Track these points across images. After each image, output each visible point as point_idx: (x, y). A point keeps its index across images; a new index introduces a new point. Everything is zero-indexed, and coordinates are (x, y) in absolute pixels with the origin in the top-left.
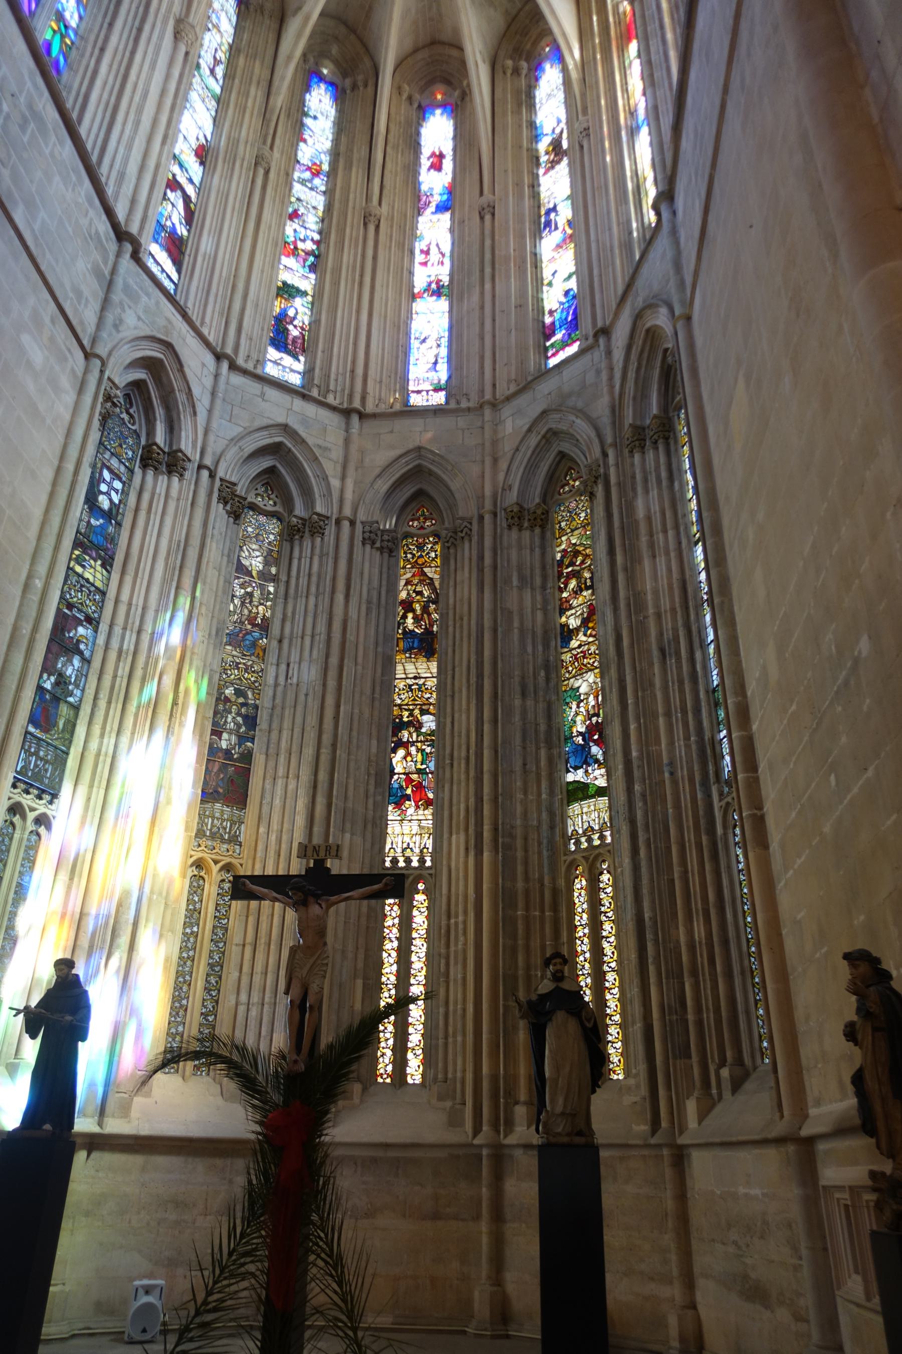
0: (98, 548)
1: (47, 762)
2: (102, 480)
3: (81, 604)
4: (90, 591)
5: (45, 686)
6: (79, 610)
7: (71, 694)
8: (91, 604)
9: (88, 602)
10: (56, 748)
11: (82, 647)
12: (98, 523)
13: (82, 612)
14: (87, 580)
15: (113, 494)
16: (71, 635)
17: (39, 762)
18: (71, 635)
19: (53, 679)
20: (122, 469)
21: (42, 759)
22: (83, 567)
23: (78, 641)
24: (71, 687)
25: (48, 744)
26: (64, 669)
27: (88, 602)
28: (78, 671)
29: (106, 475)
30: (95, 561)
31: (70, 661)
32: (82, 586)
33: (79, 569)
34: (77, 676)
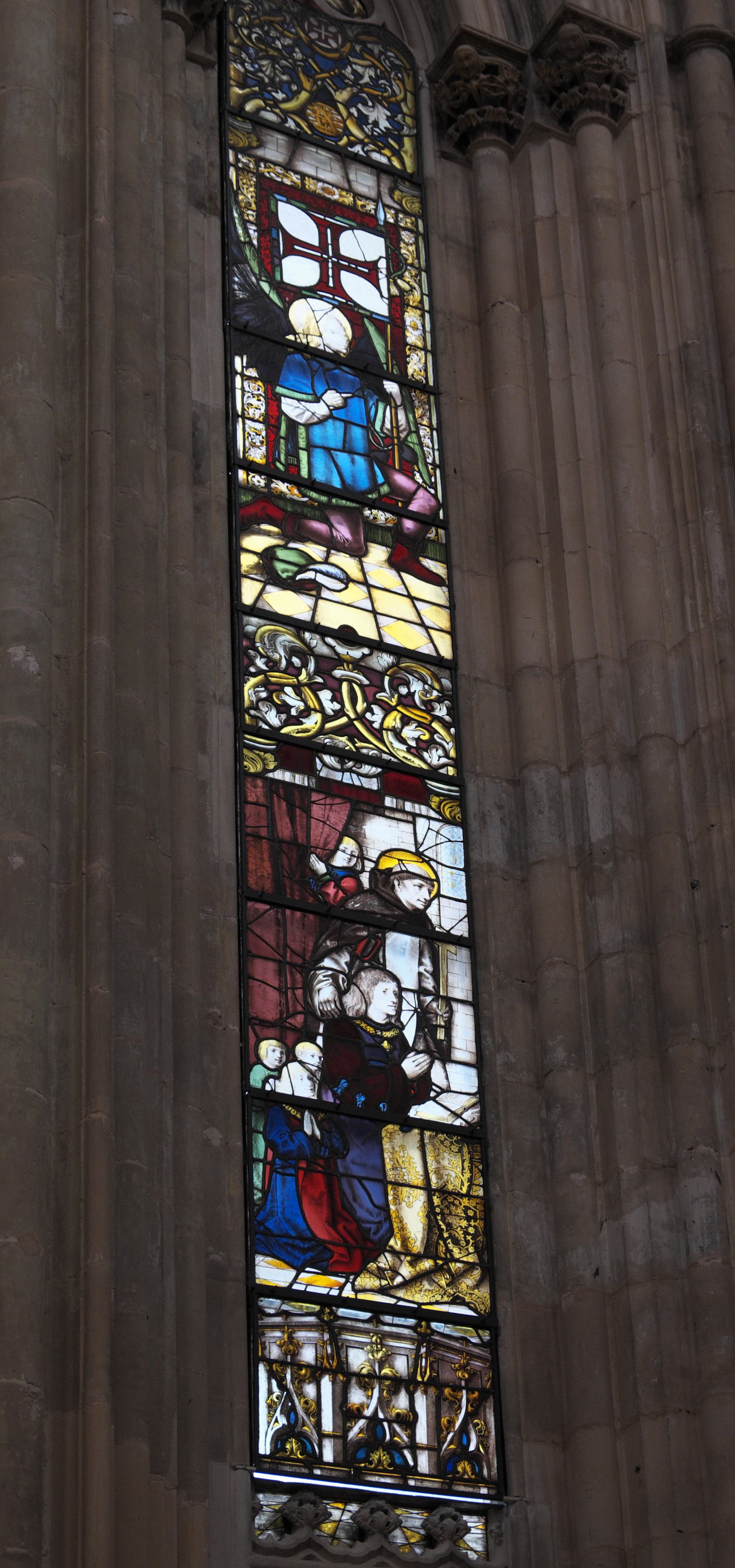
0: (352, 501)
1: (396, 1384)
2: (276, 245)
3: (347, 730)
4: (375, 676)
5: (283, 1087)
6: (342, 755)
7: (422, 1088)
8: (393, 720)
9: (376, 716)
10: (420, 1314)
11: (410, 894)
12: (321, 410)
13: (361, 759)
14: (347, 635)
15: (356, 287)
16: (340, 860)
17: (356, 1397)
18: (340, 860)
19: (309, 1052)
20: (364, 182)
21: (366, 1381)
22: (312, 589)
23: (384, 879)
25: (377, 1310)
26: (352, 1001)
27: (376, 716)
28: (421, 991)
29: (295, 221)
30: (359, 553)
31: (371, 959)
32: (326, 664)
33: (289, 603)
34: (423, 1015)
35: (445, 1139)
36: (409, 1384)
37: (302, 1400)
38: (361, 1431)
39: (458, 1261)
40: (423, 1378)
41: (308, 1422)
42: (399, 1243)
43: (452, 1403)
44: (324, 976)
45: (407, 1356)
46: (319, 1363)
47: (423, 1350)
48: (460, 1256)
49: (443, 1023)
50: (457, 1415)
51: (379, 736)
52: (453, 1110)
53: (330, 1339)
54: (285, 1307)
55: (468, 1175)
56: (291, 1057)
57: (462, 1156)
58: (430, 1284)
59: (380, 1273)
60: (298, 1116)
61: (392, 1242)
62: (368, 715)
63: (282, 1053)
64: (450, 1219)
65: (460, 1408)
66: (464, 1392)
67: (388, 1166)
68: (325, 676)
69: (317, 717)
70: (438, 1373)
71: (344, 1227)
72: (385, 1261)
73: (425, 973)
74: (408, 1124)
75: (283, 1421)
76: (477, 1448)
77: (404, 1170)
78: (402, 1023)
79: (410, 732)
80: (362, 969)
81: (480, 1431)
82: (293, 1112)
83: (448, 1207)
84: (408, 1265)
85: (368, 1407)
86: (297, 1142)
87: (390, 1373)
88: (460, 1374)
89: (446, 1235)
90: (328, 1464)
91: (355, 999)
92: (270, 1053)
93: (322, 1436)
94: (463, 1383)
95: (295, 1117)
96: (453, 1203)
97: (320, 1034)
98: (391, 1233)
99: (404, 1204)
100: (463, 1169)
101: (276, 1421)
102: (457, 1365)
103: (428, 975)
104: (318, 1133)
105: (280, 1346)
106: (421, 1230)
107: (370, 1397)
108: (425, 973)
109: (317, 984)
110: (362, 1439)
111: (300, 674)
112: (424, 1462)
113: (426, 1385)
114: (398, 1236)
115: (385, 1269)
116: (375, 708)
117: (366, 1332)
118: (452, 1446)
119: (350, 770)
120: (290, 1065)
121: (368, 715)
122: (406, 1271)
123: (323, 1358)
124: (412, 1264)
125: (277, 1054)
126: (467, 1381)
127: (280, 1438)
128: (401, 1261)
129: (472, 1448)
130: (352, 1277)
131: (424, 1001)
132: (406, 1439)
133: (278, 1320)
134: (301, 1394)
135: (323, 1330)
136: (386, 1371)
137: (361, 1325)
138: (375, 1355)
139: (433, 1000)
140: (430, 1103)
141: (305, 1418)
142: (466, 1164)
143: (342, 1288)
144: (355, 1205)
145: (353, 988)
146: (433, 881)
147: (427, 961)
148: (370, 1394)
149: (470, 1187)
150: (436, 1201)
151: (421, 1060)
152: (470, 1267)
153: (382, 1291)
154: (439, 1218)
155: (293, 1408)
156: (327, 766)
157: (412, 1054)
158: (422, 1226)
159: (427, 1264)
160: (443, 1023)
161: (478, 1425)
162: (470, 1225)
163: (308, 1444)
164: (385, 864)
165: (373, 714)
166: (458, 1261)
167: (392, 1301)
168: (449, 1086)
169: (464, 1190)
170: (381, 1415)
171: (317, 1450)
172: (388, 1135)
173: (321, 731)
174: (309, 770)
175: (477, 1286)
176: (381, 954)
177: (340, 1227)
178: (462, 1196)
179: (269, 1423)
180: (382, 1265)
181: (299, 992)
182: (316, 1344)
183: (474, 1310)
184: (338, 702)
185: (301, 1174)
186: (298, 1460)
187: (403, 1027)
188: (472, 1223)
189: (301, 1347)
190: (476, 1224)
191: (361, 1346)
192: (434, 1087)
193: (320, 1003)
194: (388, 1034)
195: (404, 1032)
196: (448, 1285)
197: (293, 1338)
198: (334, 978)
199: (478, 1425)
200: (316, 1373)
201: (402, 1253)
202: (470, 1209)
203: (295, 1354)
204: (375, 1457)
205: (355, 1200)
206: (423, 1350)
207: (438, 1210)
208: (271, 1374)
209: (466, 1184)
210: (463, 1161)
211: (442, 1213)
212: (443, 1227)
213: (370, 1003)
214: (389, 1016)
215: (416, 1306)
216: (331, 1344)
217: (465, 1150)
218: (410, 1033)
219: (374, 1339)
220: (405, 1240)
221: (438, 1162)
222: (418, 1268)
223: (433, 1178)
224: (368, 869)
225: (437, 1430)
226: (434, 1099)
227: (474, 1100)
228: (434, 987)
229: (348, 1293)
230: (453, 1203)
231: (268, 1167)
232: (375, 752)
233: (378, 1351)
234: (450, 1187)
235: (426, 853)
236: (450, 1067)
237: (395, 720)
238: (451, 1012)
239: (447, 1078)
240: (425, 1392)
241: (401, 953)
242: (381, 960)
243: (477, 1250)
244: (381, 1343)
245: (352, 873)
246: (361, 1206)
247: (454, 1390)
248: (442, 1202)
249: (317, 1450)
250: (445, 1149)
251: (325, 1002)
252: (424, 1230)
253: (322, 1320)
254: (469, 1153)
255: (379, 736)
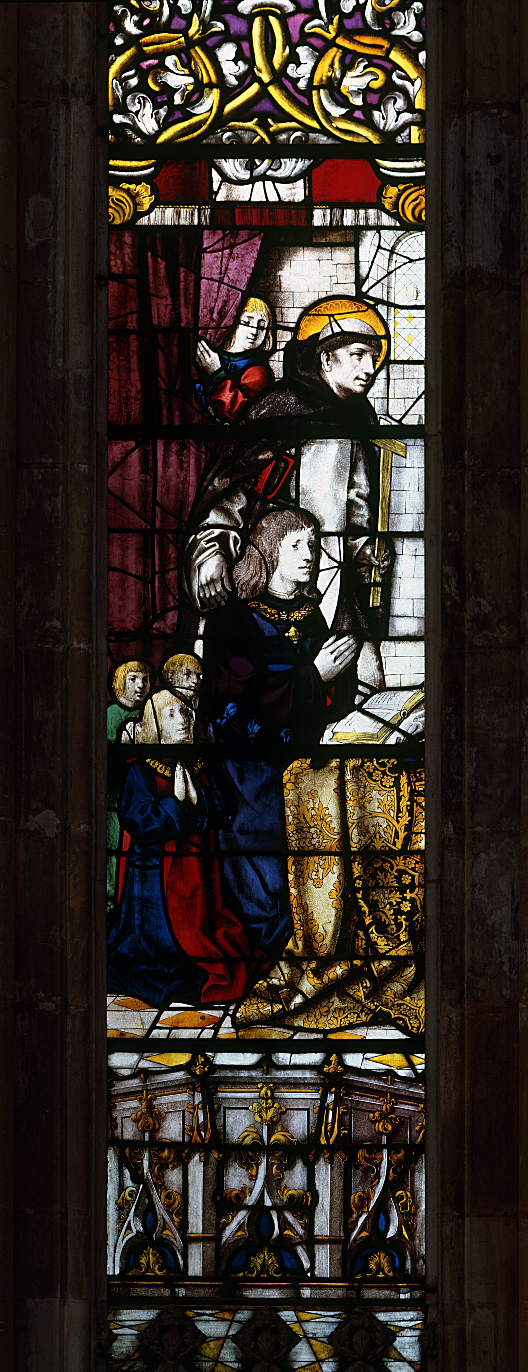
3: (260, 109)
5: (143, 733)
6: (248, 152)
7: (344, 693)
11: (344, 371)
13: (276, 151)
17: (235, 1178)
24: (326, 661)
28: (349, 531)
31: (277, 497)
35: (376, 769)
36: (306, 1151)
37: (164, 1194)
38: (240, 1227)
39: (384, 957)
40: (328, 1139)
41: (171, 1225)
42: (300, 944)
43: (367, 1171)
44: (208, 542)
45: (308, 1110)
46: (187, 1138)
47: (331, 1098)
48: (387, 948)
49: (379, 579)
50: (373, 1188)
51: (305, 101)
52: (387, 719)
53: (203, 1102)
54: (144, 1064)
55: (405, 820)
56: (157, 684)
57: (399, 790)
58: (342, 1001)
59: (273, 994)
60: (167, 774)
61: (290, 945)
62: (291, 70)
63: (144, 680)
64: (375, 896)
65: (378, 1176)
66: (385, 1152)
67: (290, 829)
68: (228, 17)
69: (213, 98)
70: (349, 1130)
71: (225, 934)
72: (281, 974)
73: (357, 499)
74: (321, 758)
75: (137, 1226)
76: (399, 1231)
77: (312, 830)
78: (319, 592)
79: (353, 82)
80: (265, 513)
81: (405, 1206)
82: (160, 768)
83: (374, 876)
84: (311, 976)
85: (251, 1192)
86: (163, 814)
87: (282, 1138)
88: (380, 1126)
89: (368, 921)
90: (195, 1278)
91: (252, 567)
92: (129, 683)
93: (188, 1240)
94: (384, 1139)
95: (162, 775)
96: (382, 870)
97: (200, 637)
98: (290, 931)
99: (310, 882)
100: (399, 811)
101: (129, 1227)
102: (377, 1114)
103: (361, 502)
104: (193, 794)
105: (136, 1121)
106: (333, 918)
107: (254, 1178)
108: (357, 499)
109: (198, 556)
110: (241, 1238)
111: (189, 25)
112: (323, 1261)
113: (332, 1150)
114: (300, 933)
115: (281, 987)
116: (303, 52)
117: (251, 1082)
118: (364, 1234)
119: (264, 178)
120: (154, 696)
121: (291, 70)
122: (308, 985)
123: (192, 1130)
124: (318, 973)
125: (139, 682)
126: (390, 1135)
127: (132, 1252)
128: (303, 972)
129: (391, 1233)
130: (232, 1007)
131: (355, 546)
132: (300, 1231)
133: (135, 1083)
134: (161, 1185)
135: (194, 1090)
136: (278, 1136)
137: (244, 1074)
138: (264, 1115)
139: (366, 544)
140: (355, 716)
141: (167, 1218)
142: (405, 803)
143: (218, 1024)
144: (241, 897)
145: (251, 549)
146: (376, 343)
147: (361, 479)
148: (254, 1173)
149: (407, 840)
150: (357, 869)
151: (342, 648)
152: (400, 963)
153: (274, 1020)
154: (360, 896)
155: (151, 1207)
156: (235, 182)
157: (332, 639)
158: (333, 912)
159: (340, 970)
160: (379, 579)
161: (402, 1197)
162: (404, 899)
163: (169, 1254)
164: (311, 328)
165: (298, 64)
166: (384, 957)
167: (287, 1034)
168: (383, 681)
169: (399, 846)
170: (268, 1202)
171: (181, 1262)
172: (292, 778)
173: (220, 121)
174: (204, 195)
175: (410, 990)
176: (293, 483)
177: (219, 934)
178: (393, 854)
179: (119, 1231)
180: (275, 981)
181: (172, 575)
182: (184, 1112)
183: (403, 1029)
184: (245, 62)
185: (168, 861)
186: (156, 1278)
187: (320, 596)
188: (408, 895)
189: (164, 1119)
190: (413, 895)
191: (243, 1105)
192: (360, 688)
193: (201, 587)
194: (297, 615)
195: (320, 606)
196: (367, 997)
197: (153, 1107)
198: (222, 540)
199: (402, 1198)
200: (180, 1153)
201: (302, 959)
202: (406, 873)
203: (154, 1130)
204: (258, 1261)
205: (241, 890)
206: (331, 1098)
207: (358, 884)
208: (123, 1162)
209: (402, 835)
210: (399, 799)
211: (365, 888)
212: (365, 909)
213: (274, 569)
214: (299, 584)
215: (320, 1036)
216: (204, 1108)
217: (404, 780)
218: (328, 608)
219: (263, 1092)
220: (309, 938)
221: (362, 808)
222: (325, 978)
223: (354, 834)
224: (282, 345)
225: (345, 1213)
226: (359, 708)
227: (421, 696)
228: (368, 521)
229: (226, 1031)
230: (382, 870)
231: (123, 860)
232: (299, 134)
233: (267, 1109)
234: (378, 844)
235: (371, 293)
236: (387, 648)
237: (332, 65)
238: (393, 557)
239: (381, 668)
240: (331, 1161)
241: (322, 473)
242: (293, 494)
243: (412, 936)
244: (272, 1097)
245: (258, 356)
246: (249, 898)
247: (370, 1153)
248: (364, 869)
249: (181, 1262)
250: (373, 784)
251: (208, 584)
252: (337, 917)
253: (193, 1074)
254: (409, 784)
255: (305, 101)
